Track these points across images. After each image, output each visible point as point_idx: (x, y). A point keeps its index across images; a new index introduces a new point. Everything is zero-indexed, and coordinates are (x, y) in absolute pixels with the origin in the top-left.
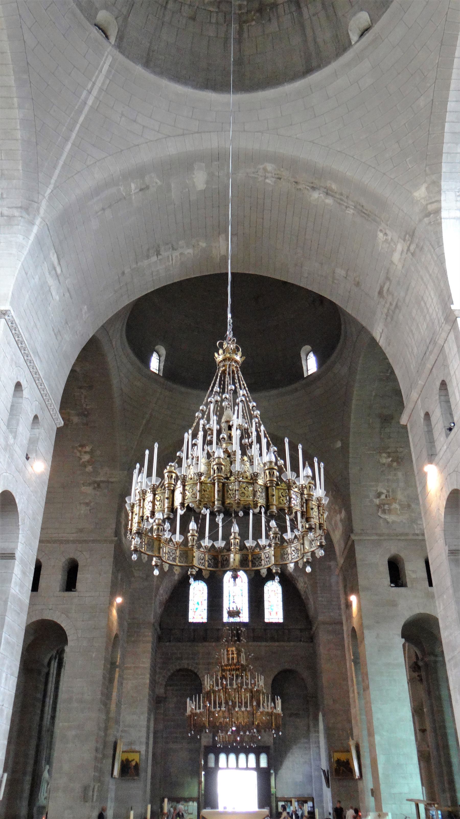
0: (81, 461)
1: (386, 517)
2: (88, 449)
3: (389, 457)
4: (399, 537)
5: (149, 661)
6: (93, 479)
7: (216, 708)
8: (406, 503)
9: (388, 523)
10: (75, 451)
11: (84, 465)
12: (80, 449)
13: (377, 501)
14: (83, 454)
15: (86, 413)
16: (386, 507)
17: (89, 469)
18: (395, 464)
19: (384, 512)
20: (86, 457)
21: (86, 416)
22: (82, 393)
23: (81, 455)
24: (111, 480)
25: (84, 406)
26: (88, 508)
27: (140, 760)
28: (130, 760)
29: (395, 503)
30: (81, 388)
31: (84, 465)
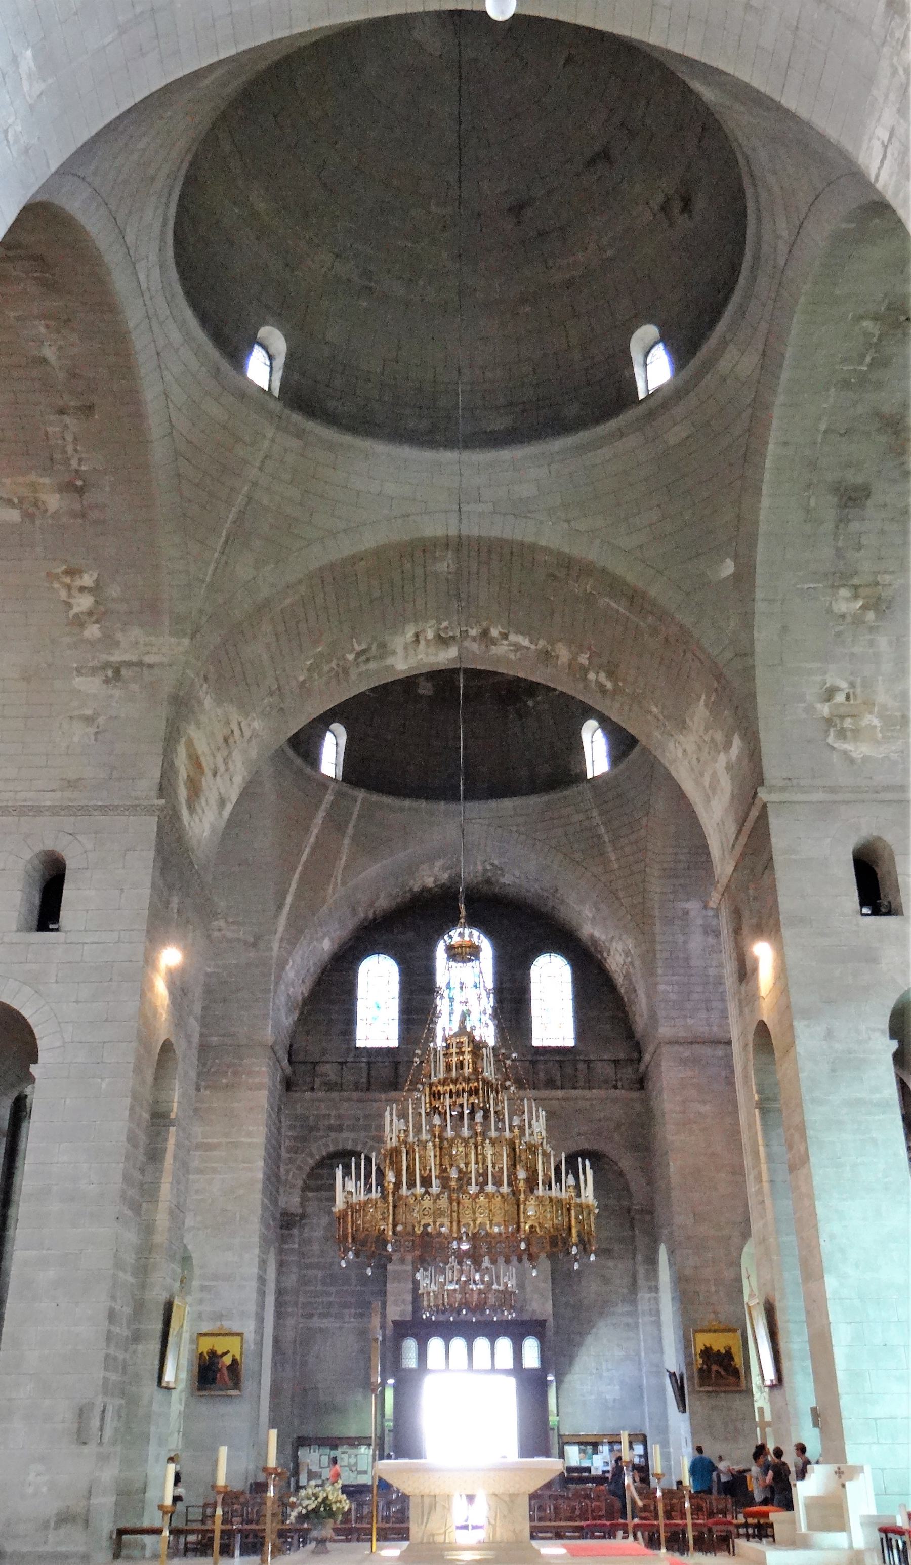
0: (71, 613)
1: (847, 746)
2: (87, 580)
3: (856, 597)
4: (880, 796)
5: (263, 1130)
6: (104, 657)
7: (415, 1185)
8: (898, 714)
9: (852, 761)
10: (56, 585)
11: (79, 622)
12: (68, 580)
13: (825, 710)
14: (75, 592)
15: (79, 483)
16: (848, 723)
17: (93, 631)
18: (871, 616)
19: (842, 734)
20: (84, 602)
21: (80, 491)
22: (66, 426)
23: (70, 595)
24: (148, 659)
25: (74, 464)
26: (92, 730)
27: (241, 1354)
28: (219, 1352)
29: (871, 713)
30: (62, 412)
31: (79, 622)
